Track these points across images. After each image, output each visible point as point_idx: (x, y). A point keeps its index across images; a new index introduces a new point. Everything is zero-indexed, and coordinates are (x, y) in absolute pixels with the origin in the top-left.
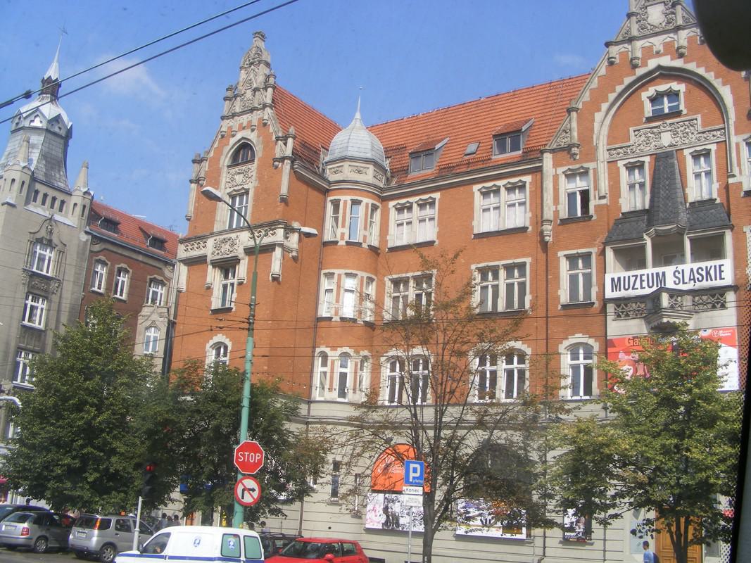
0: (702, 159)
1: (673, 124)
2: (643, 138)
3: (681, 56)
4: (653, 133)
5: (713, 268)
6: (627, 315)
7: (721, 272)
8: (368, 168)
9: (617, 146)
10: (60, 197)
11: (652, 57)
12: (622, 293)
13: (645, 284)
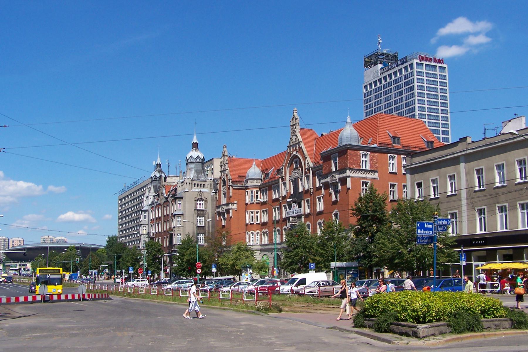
10: (203, 183)
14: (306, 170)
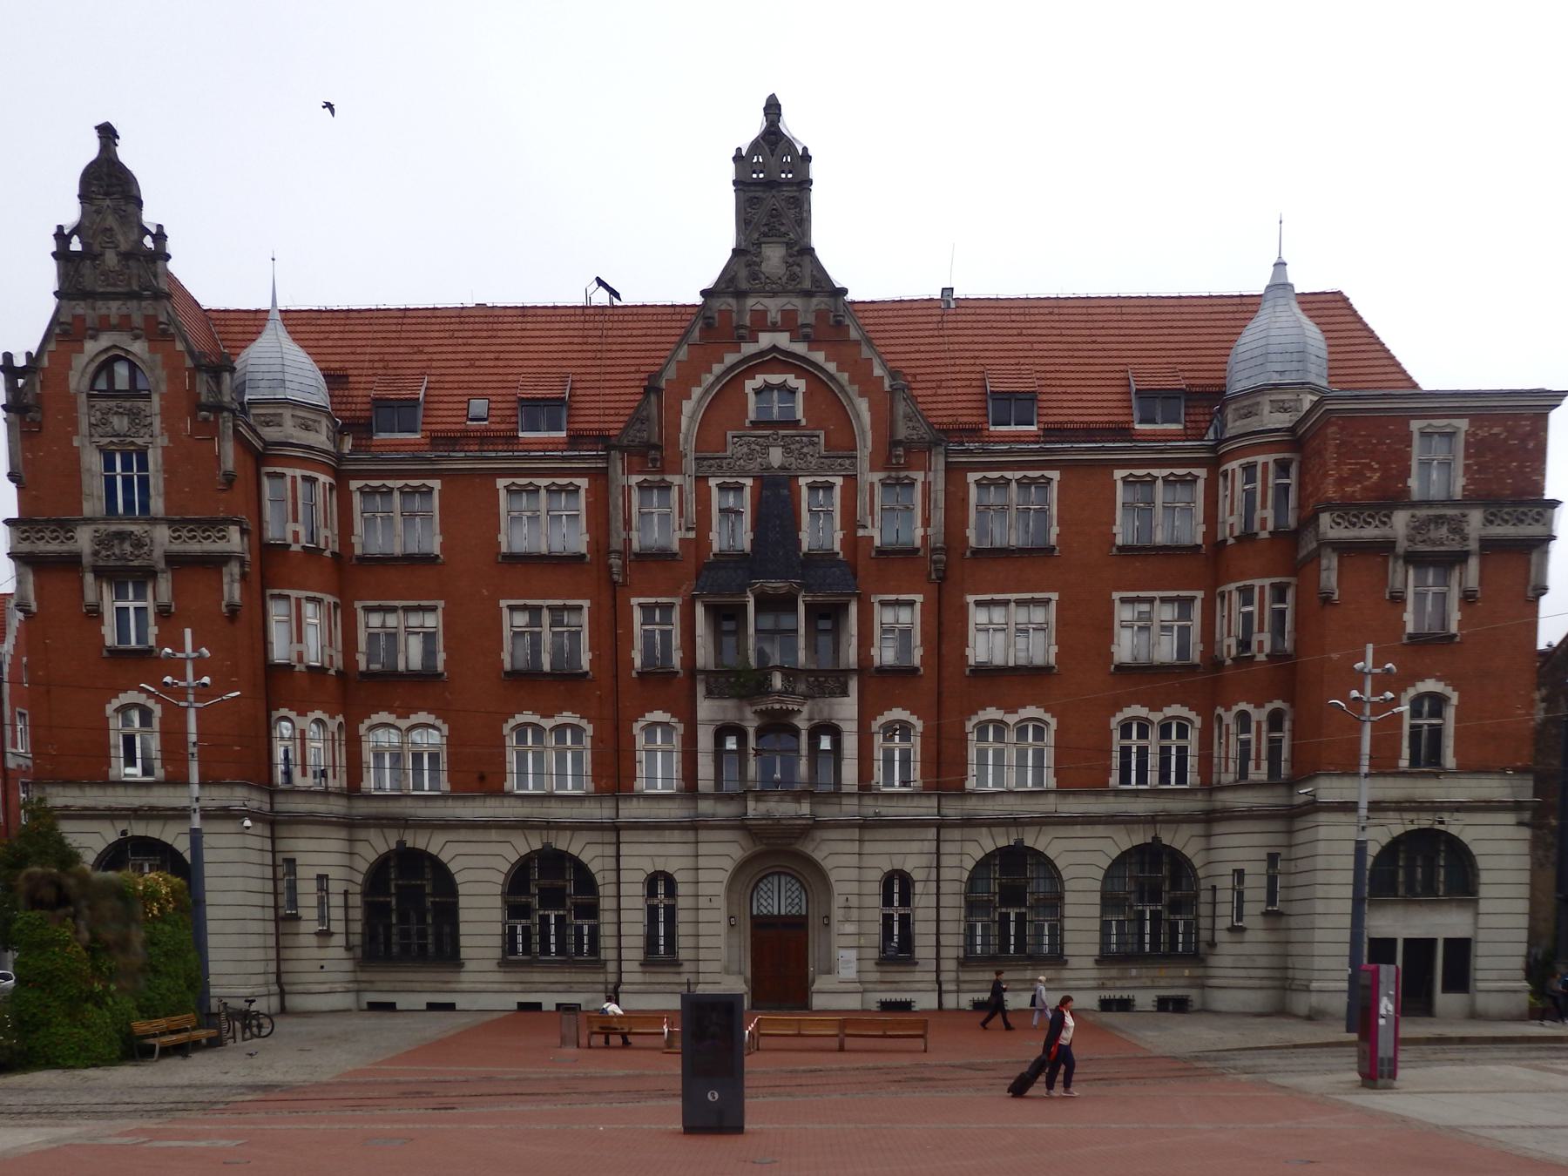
0: (821, 493)
2: (745, 450)
8: (319, 422)
14: (900, 451)
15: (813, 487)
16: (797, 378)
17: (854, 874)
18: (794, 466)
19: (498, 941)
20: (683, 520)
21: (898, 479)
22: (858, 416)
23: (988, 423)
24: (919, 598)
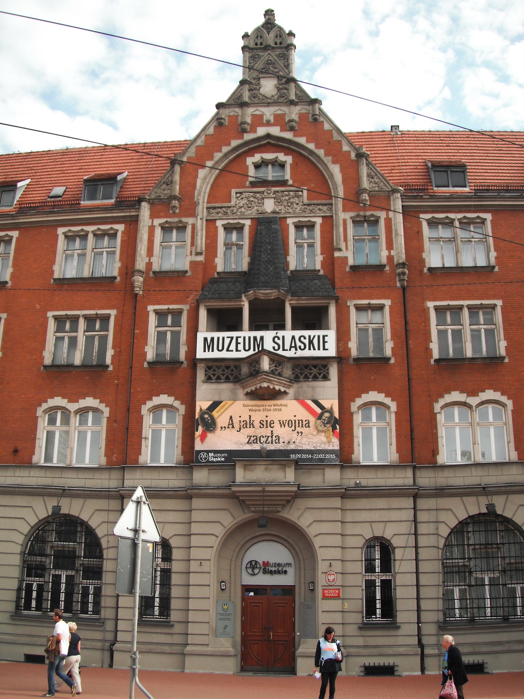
0: (305, 230)
1: (278, 192)
3: (292, 129)
4: (255, 198)
5: (316, 338)
6: (219, 378)
7: (324, 342)
9: (217, 205)
11: (262, 125)
12: (215, 354)
13: (240, 347)
14: (366, 196)
15: (299, 227)
16: (286, 154)
17: (337, 540)
18: (283, 211)
19: (13, 596)
20: (194, 248)
21: (365, 217)
22: (332, 176)
23: (432, 186)
24: (387, 303)
